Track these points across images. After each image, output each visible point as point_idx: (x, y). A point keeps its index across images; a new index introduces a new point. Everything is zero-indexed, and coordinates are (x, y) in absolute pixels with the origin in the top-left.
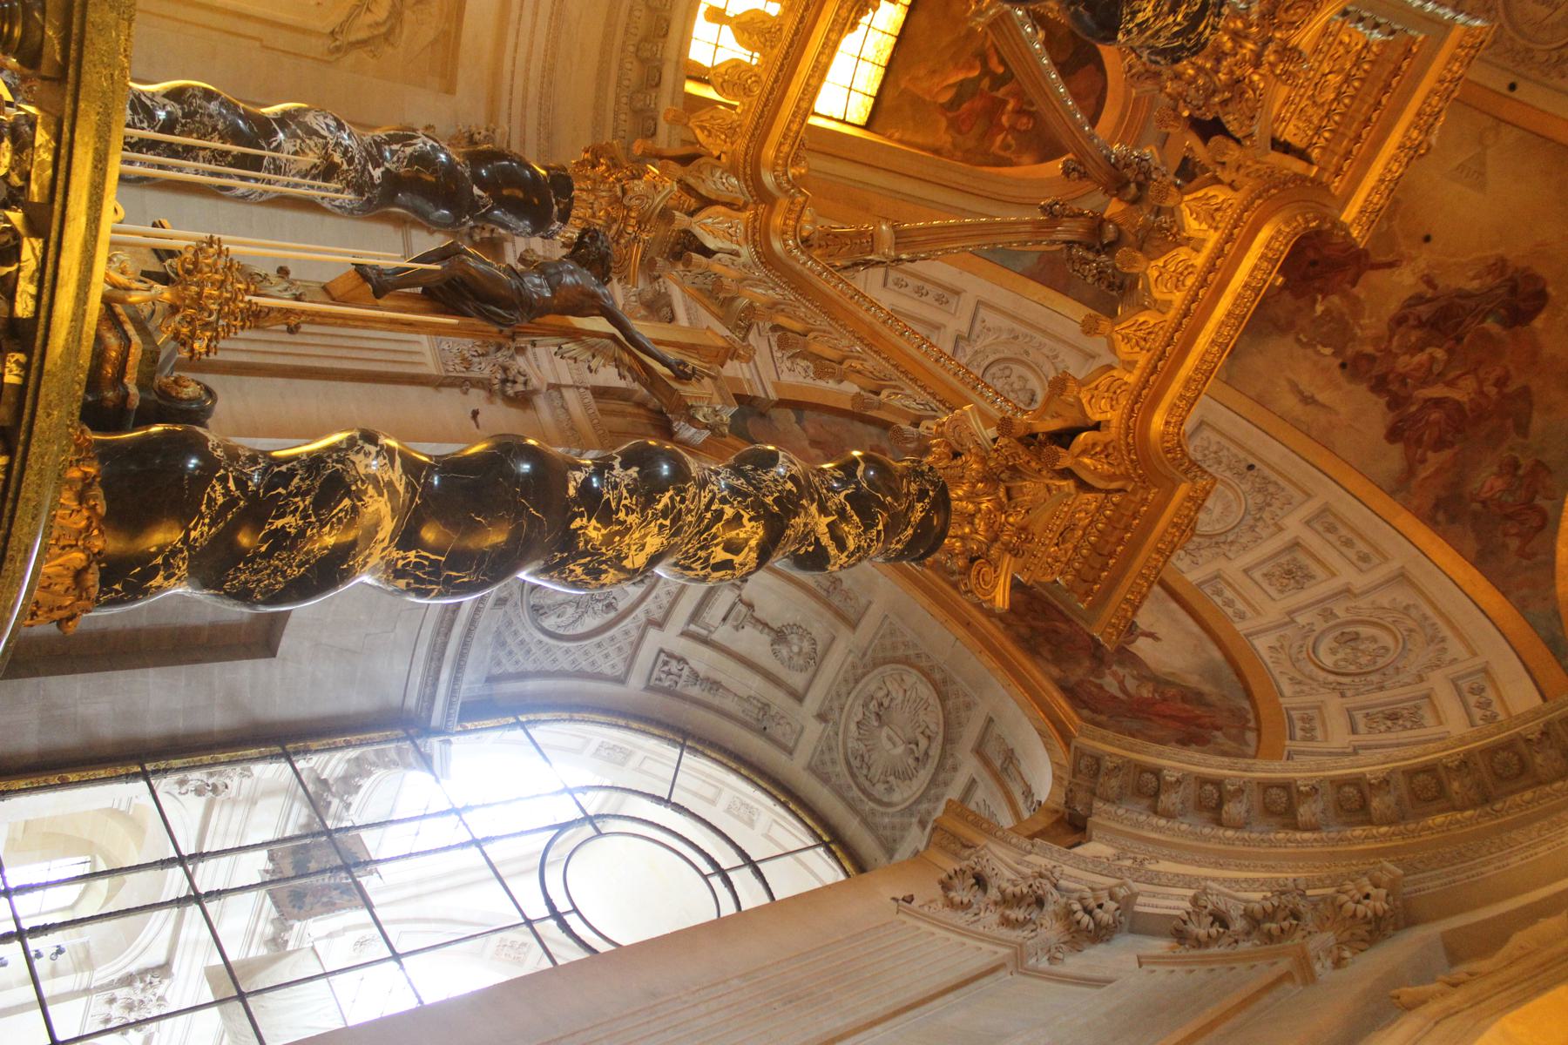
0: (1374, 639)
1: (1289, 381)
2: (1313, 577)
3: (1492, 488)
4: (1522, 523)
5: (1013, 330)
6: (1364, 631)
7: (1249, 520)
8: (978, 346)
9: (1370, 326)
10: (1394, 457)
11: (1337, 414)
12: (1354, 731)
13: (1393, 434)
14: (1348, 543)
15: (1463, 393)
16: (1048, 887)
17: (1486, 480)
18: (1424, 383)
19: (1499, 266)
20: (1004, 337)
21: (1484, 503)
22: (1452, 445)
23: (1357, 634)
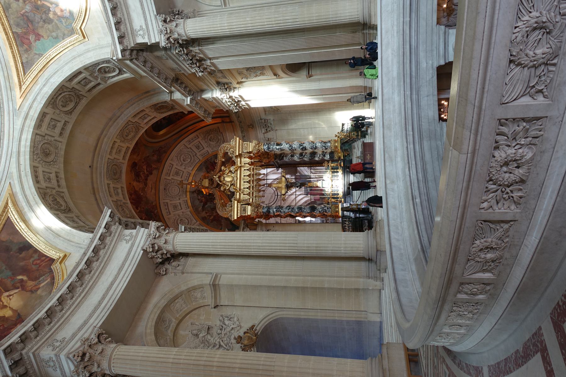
6: (182, 159)
9: (141, 185)
10: (155, 172)
13: (151, 174)
15: (145, 167)
17: (155, 158)
18: (144, 173)
19: (131, 171)
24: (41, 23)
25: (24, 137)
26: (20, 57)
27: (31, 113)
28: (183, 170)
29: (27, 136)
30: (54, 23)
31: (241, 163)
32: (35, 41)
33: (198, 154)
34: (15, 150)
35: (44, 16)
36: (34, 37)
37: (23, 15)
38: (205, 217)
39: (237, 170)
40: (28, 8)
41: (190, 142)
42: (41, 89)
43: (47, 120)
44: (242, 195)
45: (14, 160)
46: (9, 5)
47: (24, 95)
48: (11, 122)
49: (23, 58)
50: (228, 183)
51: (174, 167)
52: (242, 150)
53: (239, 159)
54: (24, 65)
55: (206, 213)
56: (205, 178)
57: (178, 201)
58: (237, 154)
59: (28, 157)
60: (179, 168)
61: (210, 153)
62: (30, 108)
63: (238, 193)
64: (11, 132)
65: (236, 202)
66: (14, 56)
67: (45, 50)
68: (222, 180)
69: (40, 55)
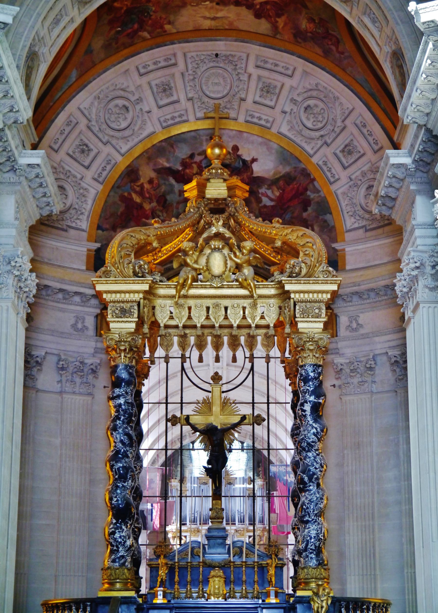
0: (316, 106)
1: (202, 17)
2: (275, 87)
3: (310, 28)
4: (331, 40)
5: (95, 98)
6: (311, 102)
7: (235, 78)
8: (94, 116)
11: (229, 17)
12: (345, 168)
13: (258, 16)
14: (276, 65)
16: (356, 364)
20: (96, 104)
21: (311, 32)
22: (283, 15)
23: (309, 106)
28: (278, 108)
31: (260, 297)
33: (327, 151)
38: (137, 179)
39: (241, 286)
41: (361, 127)
44: (169, 302)
50: (203, 261)
51: (286, 80)
52: (302, 302)
53: (273, 292)
55: (151, 181)
56: (230, 188)
57: (182, 98)
58: (287, 287)
60: (285, 92)
61: (333, 188)
63: (173, 292)
65: (146, 287)
68: (215, 243)
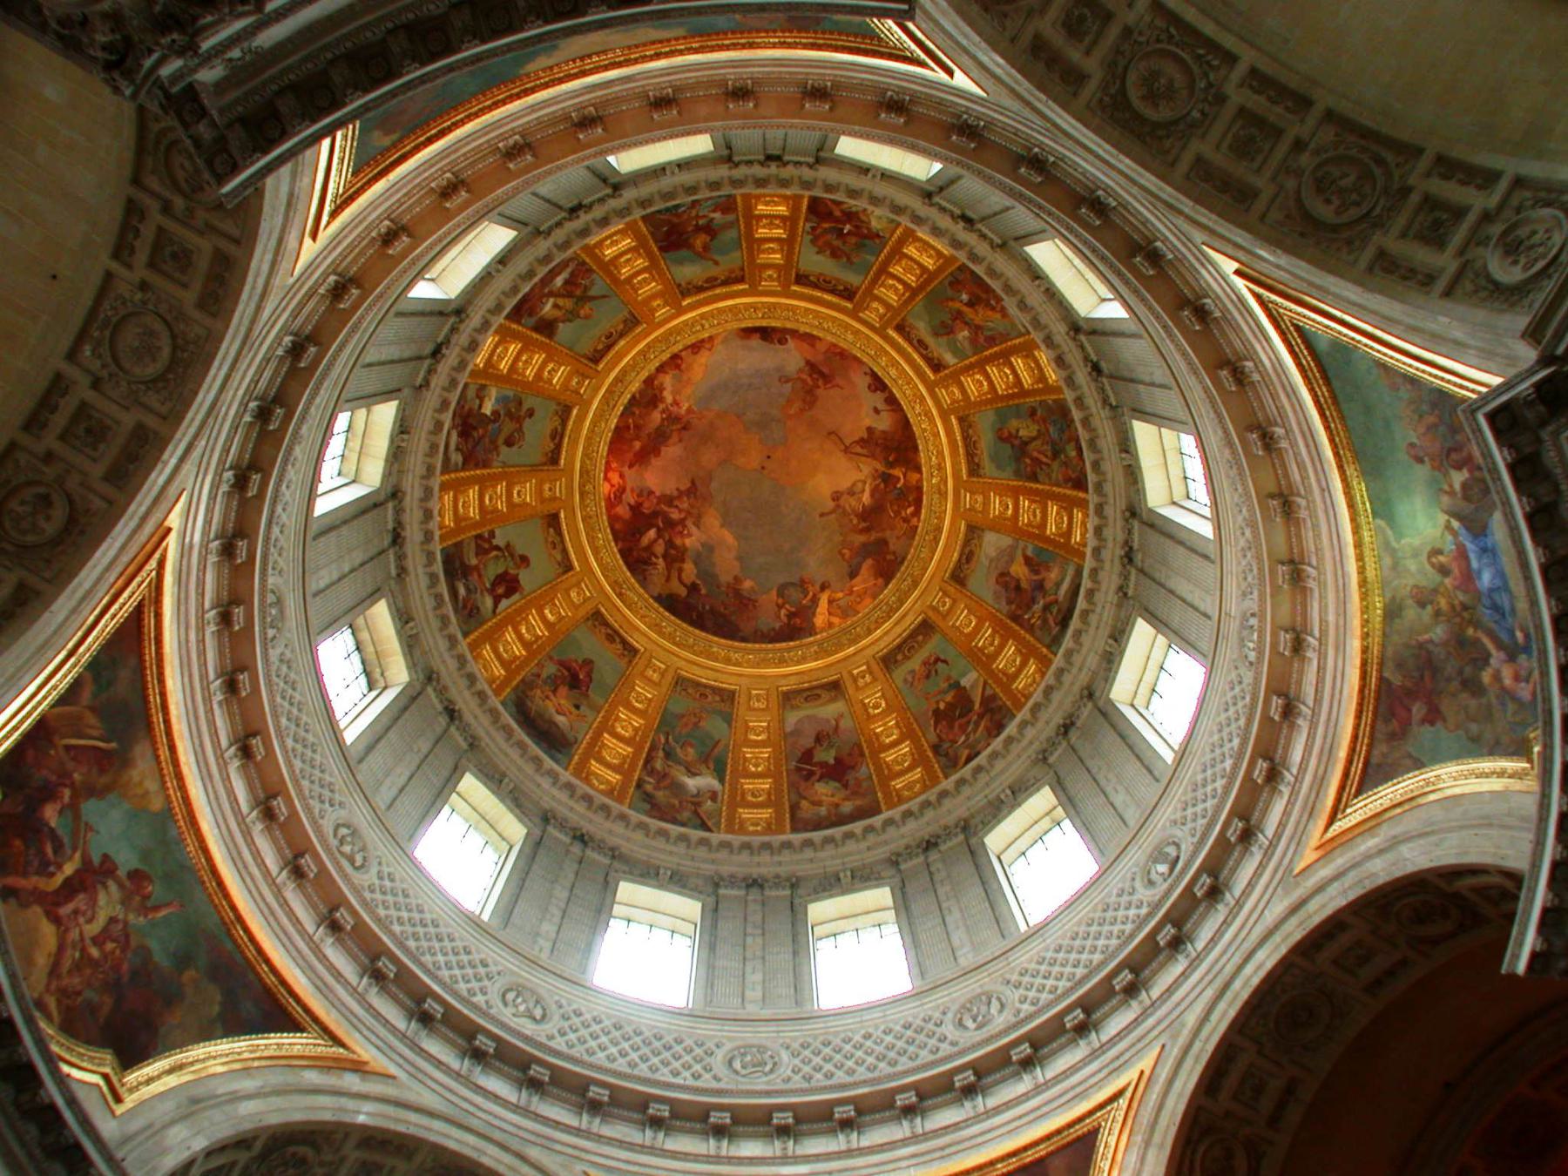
24: (1455, 685)
25: (1260, 955)
26: (1370, 746)
27: (1312, 906)
29: (1267, 959)
30: (1484, 700)
32: (1423, 721)
34: (1229, 969)
35: (1468, 670)
36: (1424, 711)
37: (1421, 646)
40: (1439, 633)
42: (1368, 857)
43: (1344, 939)
45: (1209, 993)
46: (1401, 608)
47: (1328, 848)
48: (1267, 896)
49: (1375, 752)
54: (1370, 771)
59: (1232, 1013)
62: (1320, 889)
64: (1252, 921)
66: (1355, 737)
67: (1438, 758)
69: (1419, 765)
